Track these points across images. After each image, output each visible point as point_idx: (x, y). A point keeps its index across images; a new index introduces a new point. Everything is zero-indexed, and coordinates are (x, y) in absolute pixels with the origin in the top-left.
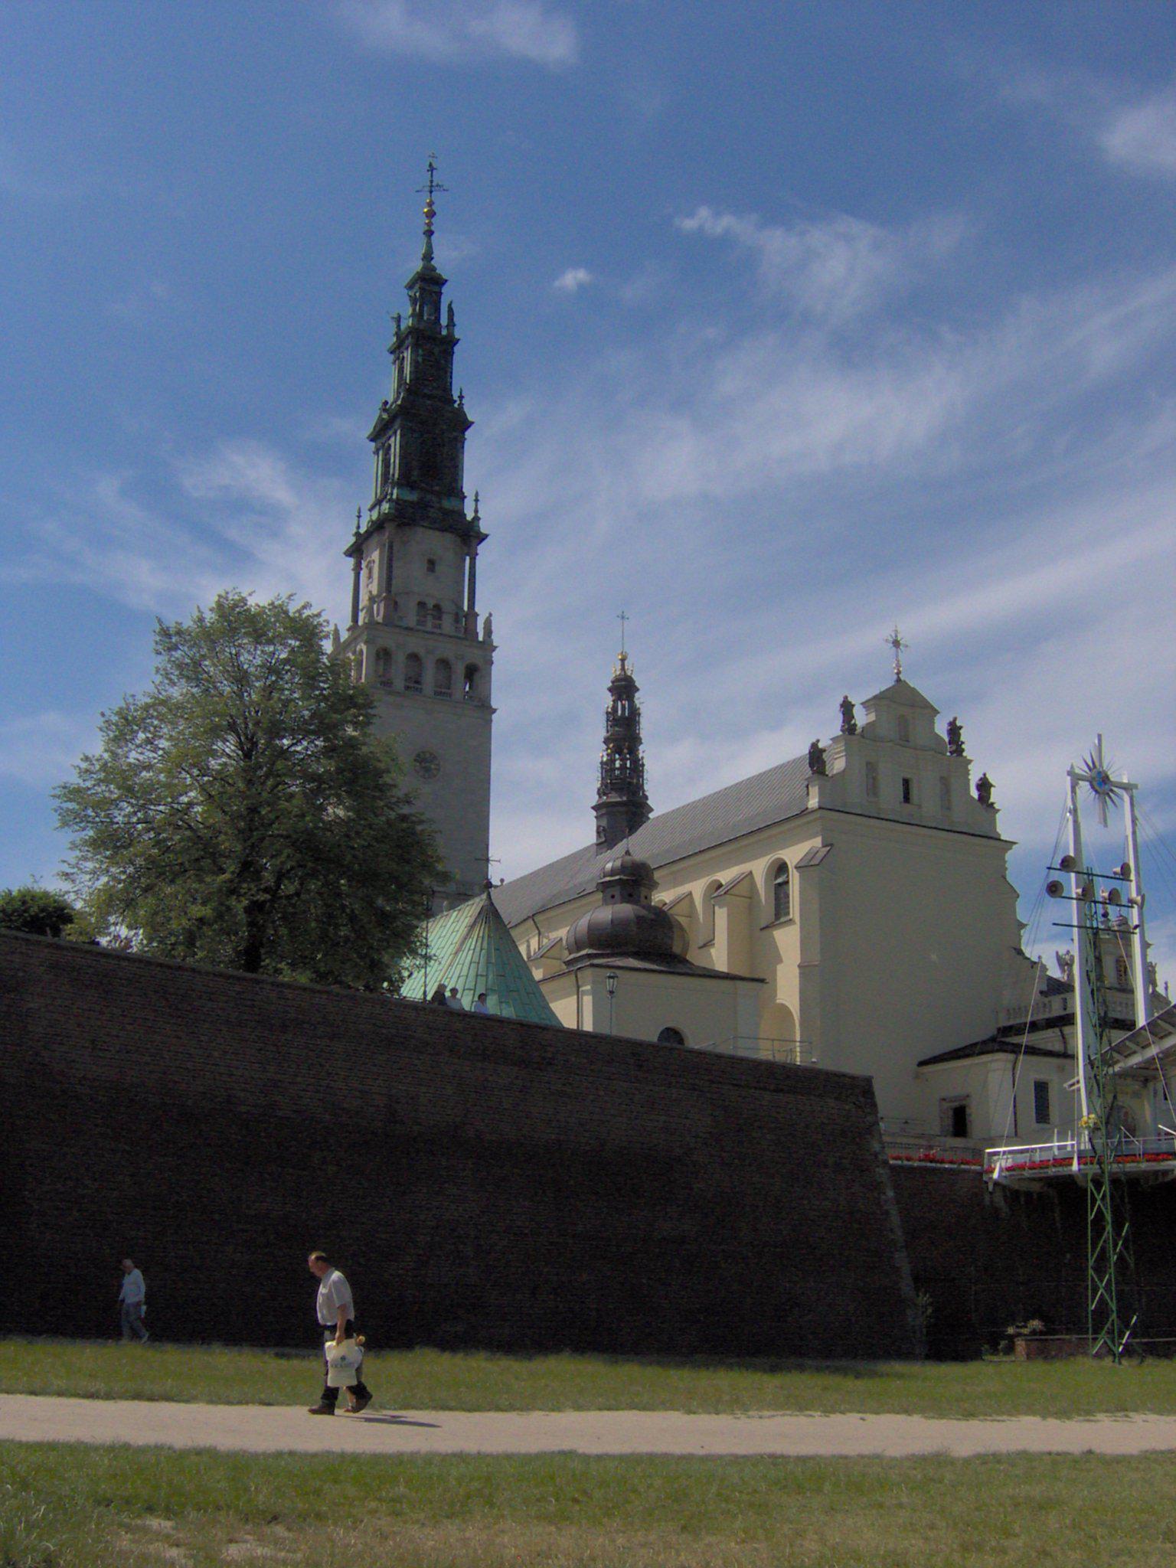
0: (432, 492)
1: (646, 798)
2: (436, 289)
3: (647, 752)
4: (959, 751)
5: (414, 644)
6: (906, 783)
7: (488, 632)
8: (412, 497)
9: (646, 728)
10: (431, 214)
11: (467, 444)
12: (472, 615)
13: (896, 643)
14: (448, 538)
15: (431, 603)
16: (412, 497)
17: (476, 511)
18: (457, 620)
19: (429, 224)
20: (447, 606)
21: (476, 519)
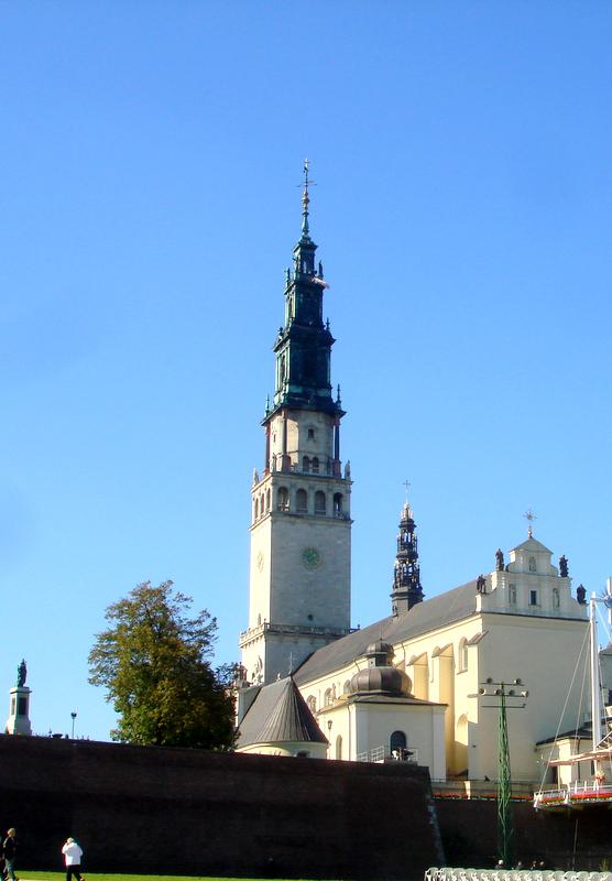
0: (311, 386)
1: (421, 588)
2: (310, 252)
3: (421, 562)
4: (565, 573)
5: (301, 484)
6: (533, 594)
7: (348, 473)
8: (299, 390)
9: (421, 549)
10: (307, 201)
11: (332, 354)
12: (337, 462)
13: (530, 517)
14: (321, 416)
15: (311, 457)
16: (299, 390)
17: (339, 397)
18: (328, 464)
19: (306, 208)
20: (322, 458)
21: (339, 401)
